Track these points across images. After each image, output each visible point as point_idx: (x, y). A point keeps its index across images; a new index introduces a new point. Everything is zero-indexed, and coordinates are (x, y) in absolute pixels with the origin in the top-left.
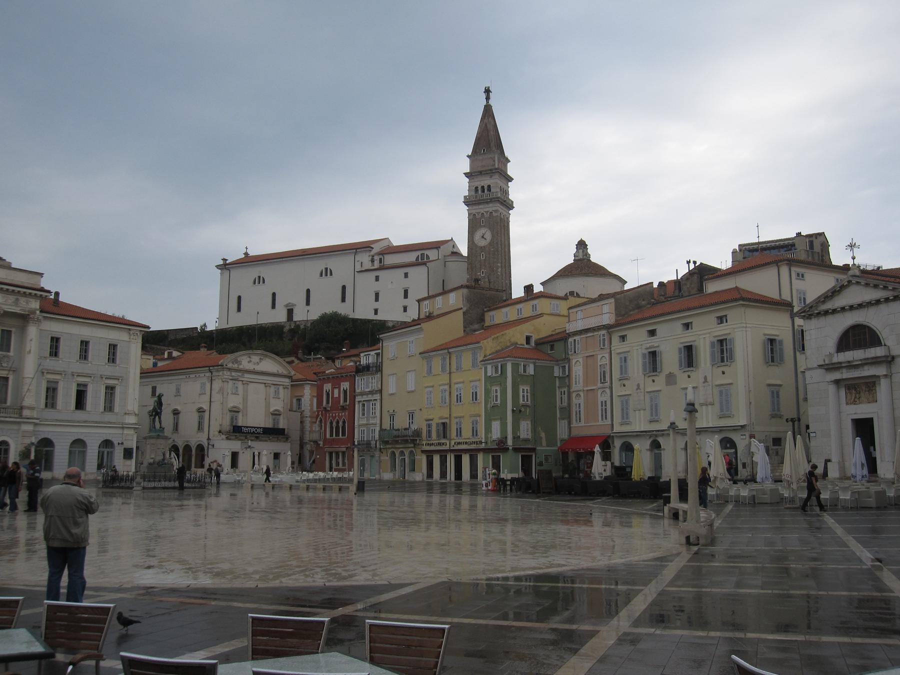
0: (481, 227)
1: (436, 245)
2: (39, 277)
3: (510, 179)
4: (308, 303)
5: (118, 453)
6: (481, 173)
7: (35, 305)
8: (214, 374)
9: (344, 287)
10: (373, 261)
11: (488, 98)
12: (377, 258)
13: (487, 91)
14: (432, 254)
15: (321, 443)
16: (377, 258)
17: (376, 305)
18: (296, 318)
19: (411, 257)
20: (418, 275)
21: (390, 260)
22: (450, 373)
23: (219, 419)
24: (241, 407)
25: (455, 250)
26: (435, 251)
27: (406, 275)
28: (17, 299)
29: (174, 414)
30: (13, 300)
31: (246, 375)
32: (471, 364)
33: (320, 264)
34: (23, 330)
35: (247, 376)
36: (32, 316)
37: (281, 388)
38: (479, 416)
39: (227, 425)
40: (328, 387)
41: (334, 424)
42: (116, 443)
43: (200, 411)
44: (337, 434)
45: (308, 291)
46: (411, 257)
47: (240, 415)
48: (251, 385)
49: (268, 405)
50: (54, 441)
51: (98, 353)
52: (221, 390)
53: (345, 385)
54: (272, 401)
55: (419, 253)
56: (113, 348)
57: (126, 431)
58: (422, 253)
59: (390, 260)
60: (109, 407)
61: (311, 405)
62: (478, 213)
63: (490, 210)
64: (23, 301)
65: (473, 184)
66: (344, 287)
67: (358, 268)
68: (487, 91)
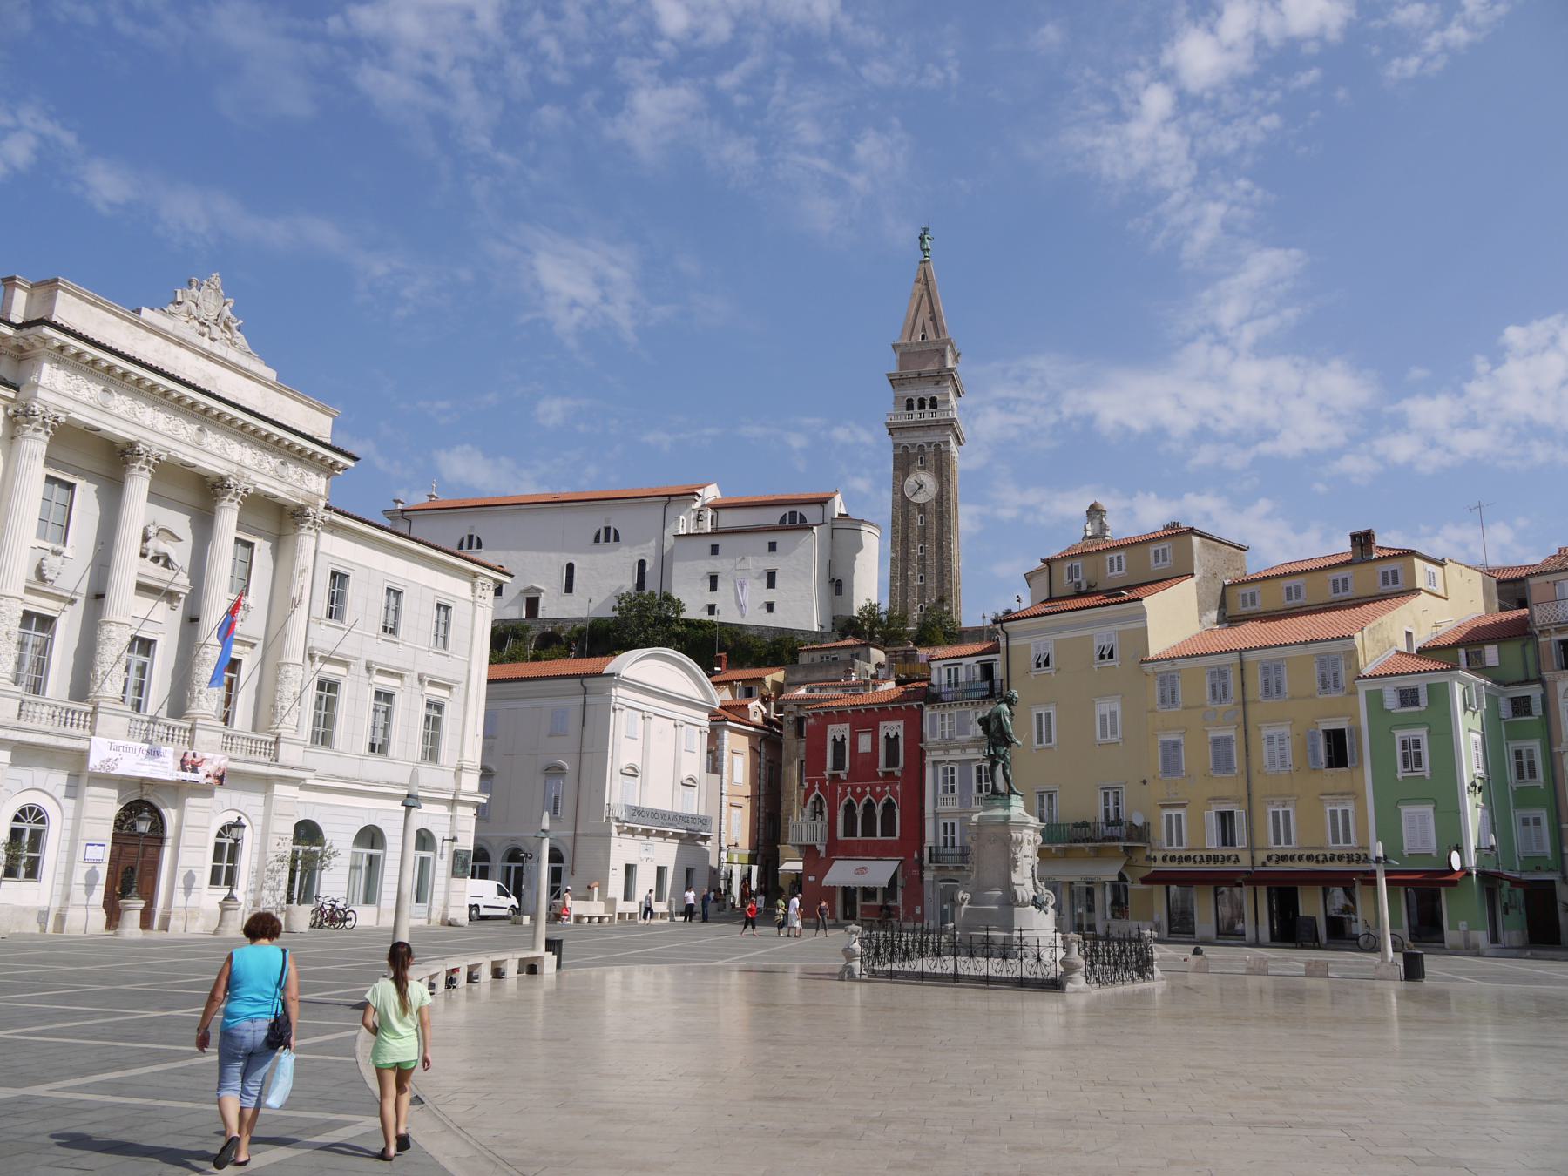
7: (316, 484)
9: (642, 564)
14: (812, 514)
15: (822, 848)
16: (709, 513)
17: (711, 598)
22: (1244, 704)
24: (638, 764)
26: (817, 509)
27: (772, 547)
32: (1317, 684)
33: (596, 520)
36: (311, 510)
38: (1356, 795)
41: (859, 811)
43: (554, 771)
44: (869, 829)
46: (773, 516)
50: (324, 828)
51: (417, 618)
53: (894, 728)
54: (685, 756)
55: (786, 510)
56: (444, 608)
57: (461, 810)
59: (728, 519)
62: (913, 445)
63: (937, 440)
65: (902, 393)
66: (642, 564)
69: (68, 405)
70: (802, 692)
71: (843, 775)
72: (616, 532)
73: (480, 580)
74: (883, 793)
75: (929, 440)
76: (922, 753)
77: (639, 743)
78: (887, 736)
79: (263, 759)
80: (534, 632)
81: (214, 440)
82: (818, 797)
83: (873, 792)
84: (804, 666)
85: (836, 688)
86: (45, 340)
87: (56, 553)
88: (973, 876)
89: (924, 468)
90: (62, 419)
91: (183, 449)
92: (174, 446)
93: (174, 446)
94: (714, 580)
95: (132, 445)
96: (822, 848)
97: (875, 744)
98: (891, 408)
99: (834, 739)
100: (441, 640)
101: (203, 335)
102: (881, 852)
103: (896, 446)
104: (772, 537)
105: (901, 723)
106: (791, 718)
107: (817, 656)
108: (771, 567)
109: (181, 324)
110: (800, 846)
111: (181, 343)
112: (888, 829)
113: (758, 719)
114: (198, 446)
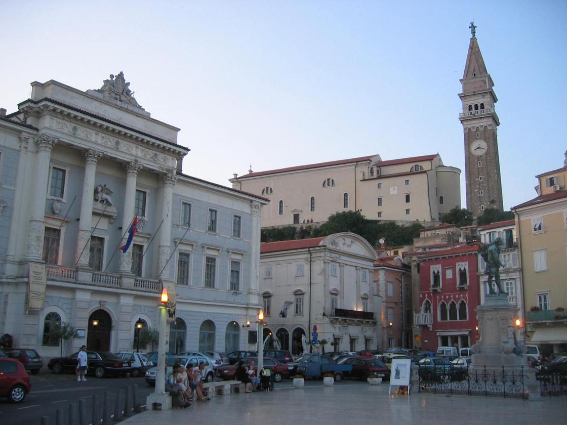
0: (477, 139)
1: (430, 158)
2: (174, 131)
3: (495, 100)
4: (312, 208)
5: (244, 336)
6: (474, 94)
8: (314, 255)
9: (346, 195)
10: (372, 173)
11: (474, 33)
12: (375, 169)
13: (473, 27)
14: (426, 166)
15: (431, 326)
16: (375, 169)
17: (380, 209)
18: (301, 221)
19: (407, 168)
20: (419, 184)
21: (386, 171)
23: (319, 302)
24: (338, 288)
25: (441, 164)
27: (407, 182)
28: (156, 155)
29: (265, 297)
30: (152, 155)
31: (343, 258)
33: (324, 175)
34: (158, 192)
35: (344, 258)
36: (170, 175)
37: (367, 271)
39: (329, 311)
40: (436, 268)
41: (448, 307)
42: (241, 325)
43: (298, 294)
44: (453, 316)
45: (312, 199)
46: (407, 168)
47: (338, 297)
48: (346, 266)
49: (358, 288)
50: (186, 322)
51: (225, 225)
52: (324, 272)
53: (463, 265)
54: (362, 284)
56: (238, 219)
58: (417, 166)
59: (386, 171)
60: (235, 286)
61: (386, 291)
62: (473, 127)
63: (485, 124)
64: (161, 156)
65: (466, 103)
66: (346, 195)
67: (360, 177)
68: (473, 27)
69: (59, 135)
70: (420, 251)
71: (439, 291)
72: (333, 180)
73: (254, 203)
74: (459, 298)
75: (481, 124)
76: (478, 277)
77: (338, 278)
78: (460, 270)
79: (154, 290)
80: (298, 230)
81: (124, 145)
82: (428, 301)
83: (454, 298)
84: (423, 238)
85: (437, 248)
86: (46, 106)
87: (58, 201)
88: (480, 340)
89: (480, 139)
90: (56, 141)
91: (110, 151)
92: (106, 150)
93: (106, 150)
94: (380, 200)
95: (87, 150)
96: (431, 326)
97: (454, 274)
98: (461, 111)
99: (434, 272)
100: (237, 233)
101: (117, 99)
102: (459, 326)
103: (465, 129)
104: (407, 178)
105: (467, 263)
106: (415, 263)
107: (429, 233)
108: (407, 192)
109: (106, 94)
110: (420, 326)
111: (107, 103)
112: (463, 316)
113: (399, 264)
114: (117, 149)
